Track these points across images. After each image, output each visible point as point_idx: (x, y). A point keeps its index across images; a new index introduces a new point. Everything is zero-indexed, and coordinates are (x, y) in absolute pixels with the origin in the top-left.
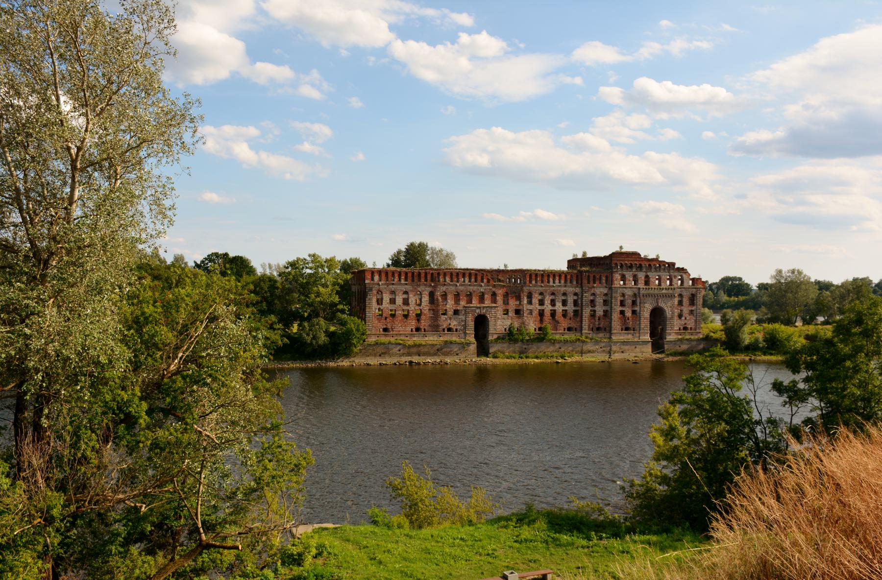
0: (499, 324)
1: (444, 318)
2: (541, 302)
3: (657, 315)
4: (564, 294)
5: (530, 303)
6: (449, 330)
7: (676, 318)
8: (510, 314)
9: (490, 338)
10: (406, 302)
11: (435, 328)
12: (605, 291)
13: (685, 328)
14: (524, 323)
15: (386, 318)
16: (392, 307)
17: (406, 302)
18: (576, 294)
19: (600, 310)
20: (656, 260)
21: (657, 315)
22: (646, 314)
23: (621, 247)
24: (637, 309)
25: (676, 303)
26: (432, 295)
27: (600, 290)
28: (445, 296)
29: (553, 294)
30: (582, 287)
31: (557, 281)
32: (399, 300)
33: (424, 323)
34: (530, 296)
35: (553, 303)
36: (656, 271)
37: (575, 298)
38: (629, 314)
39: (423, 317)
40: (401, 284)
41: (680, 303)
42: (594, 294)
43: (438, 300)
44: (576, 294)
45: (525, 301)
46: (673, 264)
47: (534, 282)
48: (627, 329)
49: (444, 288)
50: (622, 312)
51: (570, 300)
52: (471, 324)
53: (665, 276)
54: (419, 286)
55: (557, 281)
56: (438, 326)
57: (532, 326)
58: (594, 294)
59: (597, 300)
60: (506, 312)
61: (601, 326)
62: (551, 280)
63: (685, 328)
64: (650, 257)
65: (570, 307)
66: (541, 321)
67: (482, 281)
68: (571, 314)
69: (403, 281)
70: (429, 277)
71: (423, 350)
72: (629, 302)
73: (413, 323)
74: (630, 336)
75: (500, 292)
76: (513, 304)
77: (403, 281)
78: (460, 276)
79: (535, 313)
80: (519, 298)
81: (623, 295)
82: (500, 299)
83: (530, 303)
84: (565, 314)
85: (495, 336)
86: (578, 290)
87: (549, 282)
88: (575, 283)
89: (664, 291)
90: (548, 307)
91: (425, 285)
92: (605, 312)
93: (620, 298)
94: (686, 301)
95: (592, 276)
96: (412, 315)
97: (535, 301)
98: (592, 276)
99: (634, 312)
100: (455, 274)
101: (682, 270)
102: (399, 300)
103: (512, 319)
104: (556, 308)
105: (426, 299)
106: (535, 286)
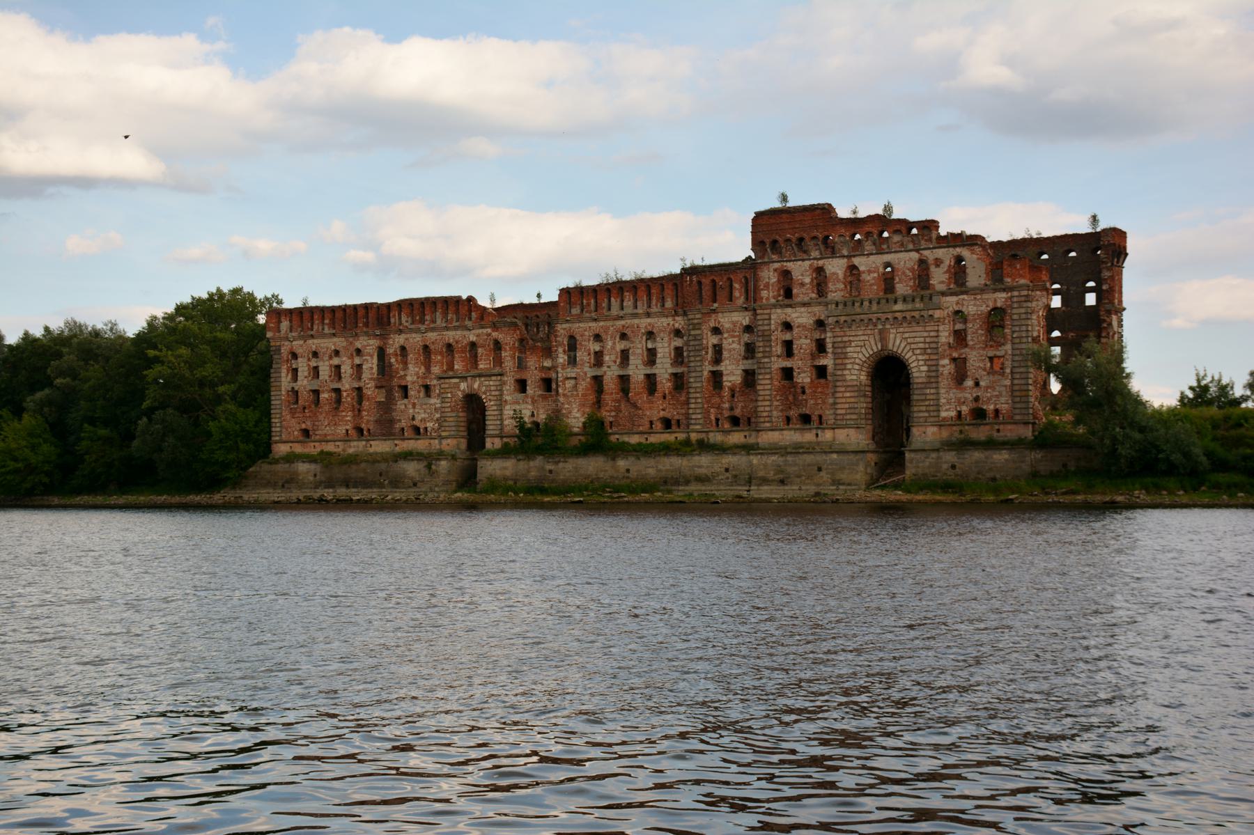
1: (401, 404)
2: (598, 358)
4: (650, 335)
5: (573, 361)
6: (417, 430)
8: (530, 391)
9: (488, 445)
11: (387, 427)
13: (979, 414)
14: (557, 412)
18: (678, 333)
19: (732, 373)
20: (881, 221)
22: (856, 373)
23: (784, 198)
25: (945, 336)
26: (382, 353)
27: (732, 319)
29: (623, 336)
30: (685, 314)
31: (628, 303)
32: (325, 372)
33: (369, 418)
34: (573, 345)
37: (678, 342)
38: (804, 378)
39: (366, 404)
40: (323, 336)
41: (960, 337)
42: (716, 331)
43: (391, 365)
44: (678, 333)
45: (562, 358)
48: (806, 419)
50: (788, 373)
51: (664, 349)
52: (455, 420)
53: (905, 260)
55: (628, 303)
56: (392, 422)
57: (576, 418)
58: (716, 331)
59: (725, 344)
60: (522, 385)
61: (737, 412)
63: (979, 414)
64: (862, 214)
65: (664, 369)
66: (598, 403)
67: (470, 319)
68: (665, 384)
69: (327, 330)
71: (354, 472)
72: (804, 344)
74: (809, 437)
75: (508, 338)
77: (327, 330)
78: (427, 309)
79: (584, 384)
80: (548, 352)
81: (788, 326)
83: (573, 361)
84: (651, 380)
85: (498, 443)
86: (679, 322)
88: (669, 304)
89: (899, 307)
90: (611, 372)
91: (367, 334)
93: (780, 336)
94: (975, 333)
95: (706, 281)
96: (347, 398)
97: (581, 355)
98: (706, 281)
102: (325, 372)
103: (534, 402)
104: (631, 371)
105: (371, 365)
106: (579, 319)
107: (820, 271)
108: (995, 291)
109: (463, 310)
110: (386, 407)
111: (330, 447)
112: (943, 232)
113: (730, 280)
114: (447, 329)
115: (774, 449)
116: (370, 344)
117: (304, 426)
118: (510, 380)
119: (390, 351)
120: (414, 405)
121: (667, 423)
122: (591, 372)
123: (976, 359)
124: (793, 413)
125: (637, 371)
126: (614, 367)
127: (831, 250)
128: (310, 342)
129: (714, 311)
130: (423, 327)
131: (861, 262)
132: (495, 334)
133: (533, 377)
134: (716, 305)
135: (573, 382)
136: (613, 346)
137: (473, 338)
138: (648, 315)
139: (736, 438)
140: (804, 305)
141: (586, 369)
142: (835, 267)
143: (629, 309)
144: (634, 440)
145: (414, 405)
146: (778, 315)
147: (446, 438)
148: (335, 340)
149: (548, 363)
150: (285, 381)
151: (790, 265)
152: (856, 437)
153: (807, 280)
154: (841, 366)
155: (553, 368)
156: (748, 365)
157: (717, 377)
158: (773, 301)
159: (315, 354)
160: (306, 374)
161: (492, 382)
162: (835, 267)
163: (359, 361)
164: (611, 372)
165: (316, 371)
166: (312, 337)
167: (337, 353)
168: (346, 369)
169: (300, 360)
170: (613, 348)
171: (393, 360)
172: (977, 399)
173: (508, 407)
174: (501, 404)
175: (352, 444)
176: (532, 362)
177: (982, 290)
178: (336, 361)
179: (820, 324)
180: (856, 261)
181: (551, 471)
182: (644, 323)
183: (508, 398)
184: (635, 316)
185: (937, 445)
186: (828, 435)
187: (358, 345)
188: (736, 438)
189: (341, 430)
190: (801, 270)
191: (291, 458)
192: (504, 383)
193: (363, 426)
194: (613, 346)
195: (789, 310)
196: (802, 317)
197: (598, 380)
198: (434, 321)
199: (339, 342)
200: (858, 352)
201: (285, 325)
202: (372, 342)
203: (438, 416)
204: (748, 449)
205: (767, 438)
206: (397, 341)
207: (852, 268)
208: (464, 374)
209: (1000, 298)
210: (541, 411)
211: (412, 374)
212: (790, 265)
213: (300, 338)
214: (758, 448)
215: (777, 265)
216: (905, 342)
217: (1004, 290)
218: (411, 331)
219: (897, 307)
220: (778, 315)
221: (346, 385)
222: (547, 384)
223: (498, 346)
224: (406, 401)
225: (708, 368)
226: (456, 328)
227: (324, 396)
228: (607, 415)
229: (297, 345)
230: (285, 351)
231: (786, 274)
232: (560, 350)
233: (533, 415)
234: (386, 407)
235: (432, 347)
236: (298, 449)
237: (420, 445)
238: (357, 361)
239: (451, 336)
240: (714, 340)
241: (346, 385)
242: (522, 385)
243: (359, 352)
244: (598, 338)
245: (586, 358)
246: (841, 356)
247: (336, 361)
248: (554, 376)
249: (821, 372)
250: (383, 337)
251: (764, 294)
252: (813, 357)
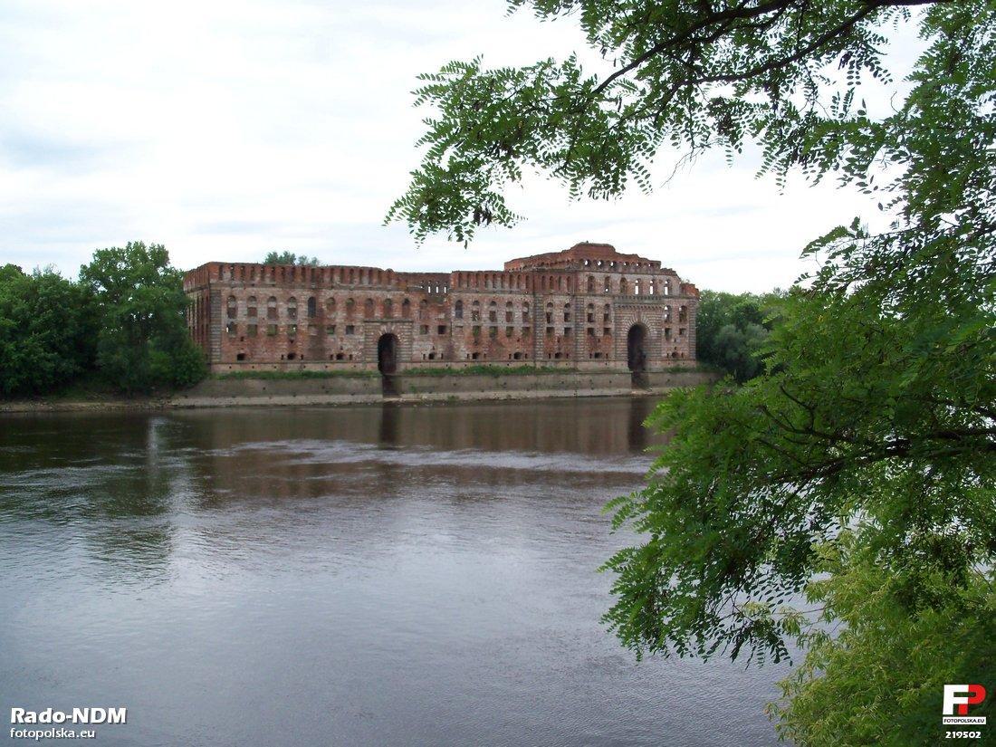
0: (416, 348)
1: (330, 338)
2: (476, 315)
3: (637, 333)
4: (510, 304)
5: (459, 316)
7: (664, 339)
10: (273, 313)
11: (318, 353)
12: (567, 300)
15: (242, 339)
16: (253, 321)
17: (273, 313)
18: (526, 304)
19: (559, 328)
21: (637, 333)
22: (624, 334)
24: (612, 326)
26: (312, 302)
27: (560, 300)
28: (332, 303)
29: (493, 303)
30: (534, 294)
31: (499, 283)
32: (262, 311)
33: (302, 347)
35: (493, 316)
36: (636, 273)
37: (526, 310)
38: (600, 334)
40: (266, 286)
42: (550, 305)
43: (322, 310)
44: (526, 304)
46: (658, 263)
47: (465, 286)
48: (597, 355)
49: (330, 293)
50: (590, 331)
51: (518, 314)
52: (374, 349)
53: (648, 278)
54: (293, 288)
55: (499, 283)
56: (322, 350)
60: (425, 329)
61: (562, 351)
62: (490, 283)
65: (518, 324)
66: (477, 343)
68: (518, 332)
69: (268, 281)
70: (308, 274)
72: (599, 316)
73: (283, 348)
75: (415, 299)
76: (435, 318)
77: (268, 281)
78: (356, 274)
79: (468, 332)
81: (591, 306)
82: (415, 310)
83: (459, 316)
85: (410, 366)
87: (486, 285)
88: (524, 287)
89: (646, 301)
90: (486, 324)
91: (303, 287)
92: (567, 330)
94: (675, 318)
95: (548, 277)
97: (467, 313)
98: (548, 277)
99: (607, 330)
100: (347, 271)
101: (671, 273)
102: (262, 311)
105: (303, 309)
106: (468, 291)
107: (607, 279)
108: (684, 298)
109: (385, 279)
110: (318, 339)
111: (268, 368)
112: (662, 267)
113: (560, 278)
114: (370, 289)
116: (303, 295)
117: (242, 352)
118: (417, 325)
119: (322, 300)
120: (342, 340)
121: (517, 356)
122: (472, 324)
123: (675, 330)
124: (593, 353)
125: (502, 324)
126: (489, 321)
127: (614, 269)
128: (250, 289)
129: (551, 294)
130: (352, 286)
131: (629, 278)
132: (407, 295)
134: (553, 291)
135: (458, 329)
136: (486, 309)
137: (389, 296)
138: (511, 292)
139: (562, 365)
140: (602, 295)
141: (470, 321)
142: (616, 277)
143: (499, 287)
144: (502, 365)
145: (342, 340)
146: (587, 300)
147: (370, 362)
148: (274, 289)
149: (442, 316)
150: (225, 318)
151: (595, 274)
152: (623, 366)
153: (602, 282)
154: (618, 329)
155: (448, 319)
156: (567, 325)
157: (550, 330)
158: (586, 292)
159: (253, 298)
160: (246, 313)
161: (406, 326)
162: (616, 277)
163: (289, 308)
164: (486, 324)
165: (252, 312)
166: (253, 285)
167: (273, 299)
168: (283, 309)
169: (239, 302)
170: (487, 310)
171: (324, 307)
172: (675, 348)
173: (415, 343)
174: (411, 340)
175: (288, 365)
177: (679, 297)
178: (272, 305)
179: (607, 306)
180: (626, 276)
181: (455, 385)
182: (507, 297)
183: (416, 337)
184: (503, 292)
185: (662, 370)
186: (612, 365)
187: (294, 294)
188: (562, 365)
189: (278, 356)
190: (599, 277)
191: (233, 376)
192: (413, 327)
193: (298, 352)
194: (486, 309)
195: (593, 298)
196: (599, 302)
197: (477, 328)
198: (361, 282)
199: (277, 291)
200: (627, 324)
201: (227, 275)
202: (305, 293)
203: (361, 347)
204: (574, 370)
205: (582, 366)
206: (327, 294)
208: (385, 320)
209: (685, 302)
210: (439, 346)
211: (339, 317)
212: (595, 274)
213: (241, 286)
214: (578, 371)
215: (588, 273)
217: (688, 298)
218: (341, 288)
219: (646, 301)
220: (587, 300)
221: (283, 322)
222: (442, 329)
223: (407, 302)
224: (335, 336)
225: (547, 325)
226: (377, 289)
227: (263, 330)
228: (483, 350)
229: (237, 291)
230: (226, 292)
231: (591, 278)
232: (453, 308)
233: (434, 349)
234: (318, 339)
235: (358, 301)
236: (238, 368)
237: (348, 367)
238: (292, 305)
239: (373, 294)
240: (548, 310)
241: (283, 322)
242: (425, 329)
243: (293, 299)
244: (476, 303)
245: (471, 315)
246: (618, 323)
247: (272, 305)
248: (449, 324)
249: (607, 330)
251: (581, 287)
252: (605, 324)
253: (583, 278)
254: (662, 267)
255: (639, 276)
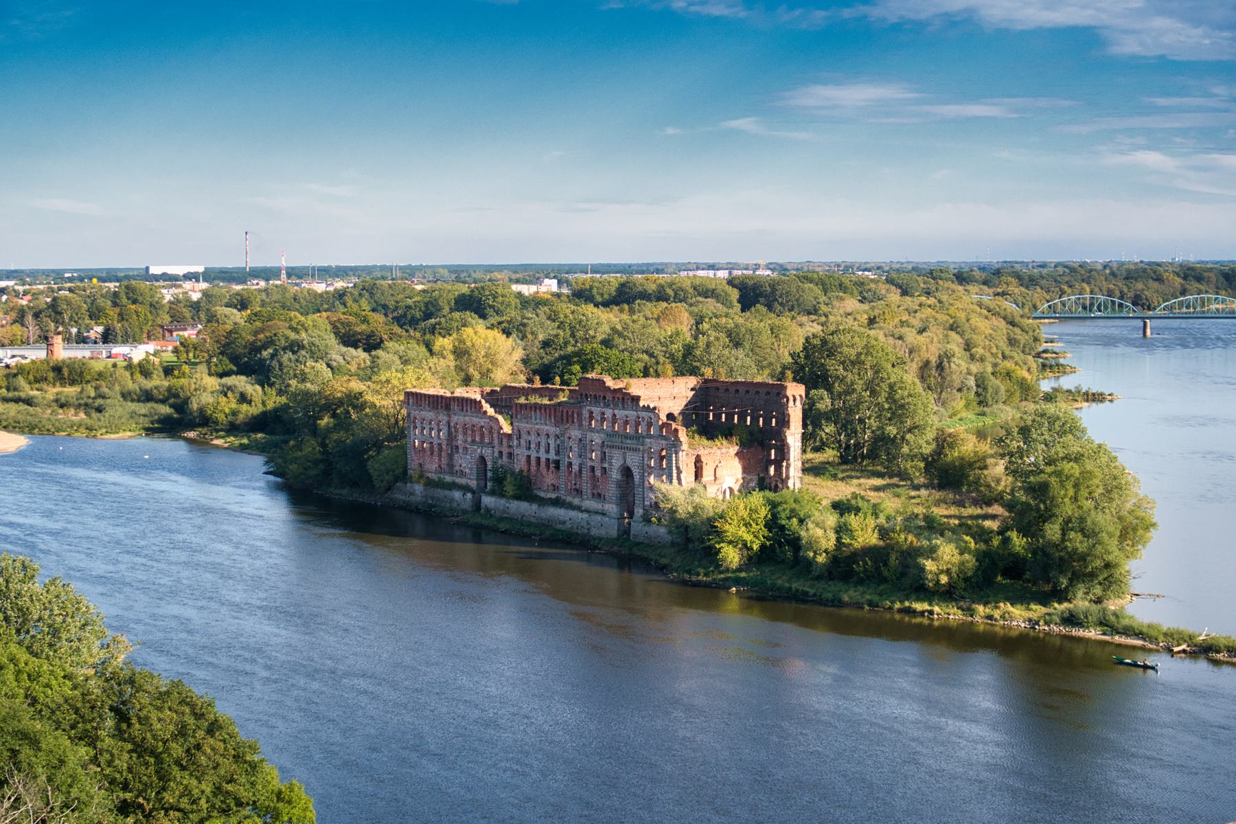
22: (615, 475)
56: (453, 466)
79: (524, 459)
90: (534, 455)
110: (451, 457)
115: (587, 511)
118: (496, 450)
125: (543, 457)
133: (505, 450)
176: (505, 442)
180: (616, 412)
197: (529, 457)
200: (617, 463)
207: (614, 415)
216: (633, 461)
231: (591, 413)
246: (610, 464)
250: (449, 416)
253: (585, 414)
254: (641, 404)
255: (626, 412)
